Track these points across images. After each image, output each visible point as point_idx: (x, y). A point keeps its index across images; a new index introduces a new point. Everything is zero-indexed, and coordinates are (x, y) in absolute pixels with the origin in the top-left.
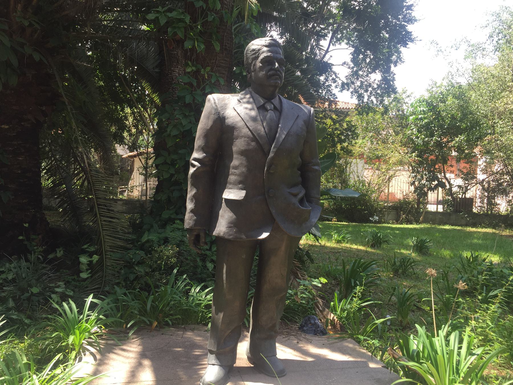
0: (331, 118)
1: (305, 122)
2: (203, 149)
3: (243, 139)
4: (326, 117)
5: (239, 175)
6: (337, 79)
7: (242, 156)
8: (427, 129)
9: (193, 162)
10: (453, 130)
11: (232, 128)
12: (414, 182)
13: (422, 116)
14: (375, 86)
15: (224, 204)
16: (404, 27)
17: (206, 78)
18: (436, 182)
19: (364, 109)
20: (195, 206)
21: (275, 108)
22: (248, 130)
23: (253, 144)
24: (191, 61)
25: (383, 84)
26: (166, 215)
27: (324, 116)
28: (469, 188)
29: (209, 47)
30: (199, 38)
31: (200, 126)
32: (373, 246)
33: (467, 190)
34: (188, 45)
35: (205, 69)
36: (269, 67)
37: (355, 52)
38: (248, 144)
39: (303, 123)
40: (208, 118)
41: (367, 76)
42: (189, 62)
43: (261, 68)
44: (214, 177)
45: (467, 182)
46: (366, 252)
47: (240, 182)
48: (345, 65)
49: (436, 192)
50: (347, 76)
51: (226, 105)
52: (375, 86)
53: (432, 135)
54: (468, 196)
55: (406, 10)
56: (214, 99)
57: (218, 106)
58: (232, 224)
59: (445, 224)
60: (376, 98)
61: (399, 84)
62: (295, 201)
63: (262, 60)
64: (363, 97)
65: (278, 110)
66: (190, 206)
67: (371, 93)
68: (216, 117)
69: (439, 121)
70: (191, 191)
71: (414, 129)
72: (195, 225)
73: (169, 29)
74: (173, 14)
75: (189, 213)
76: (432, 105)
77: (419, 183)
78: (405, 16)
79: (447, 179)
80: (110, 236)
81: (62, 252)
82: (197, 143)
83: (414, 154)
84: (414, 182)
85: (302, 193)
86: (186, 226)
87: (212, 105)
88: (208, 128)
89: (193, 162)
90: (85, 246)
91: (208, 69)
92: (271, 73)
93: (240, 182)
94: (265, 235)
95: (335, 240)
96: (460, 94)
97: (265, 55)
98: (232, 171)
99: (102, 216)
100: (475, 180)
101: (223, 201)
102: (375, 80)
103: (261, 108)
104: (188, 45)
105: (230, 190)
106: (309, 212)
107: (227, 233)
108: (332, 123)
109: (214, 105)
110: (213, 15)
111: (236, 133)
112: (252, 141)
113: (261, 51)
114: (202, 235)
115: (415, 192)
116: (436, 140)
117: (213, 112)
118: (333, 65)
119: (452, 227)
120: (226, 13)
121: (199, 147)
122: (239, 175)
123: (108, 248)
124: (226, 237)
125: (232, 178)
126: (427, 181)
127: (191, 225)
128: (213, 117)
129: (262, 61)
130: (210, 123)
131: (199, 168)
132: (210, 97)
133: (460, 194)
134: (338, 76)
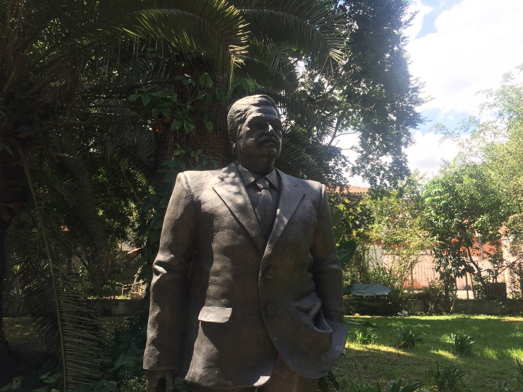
0: (344, 203)
1: (314, 202)
2: (170, 248)
3: (226, 231)
4: (338, 202)
5: (221, 285)
6: (347, 163)
7: (225, 255)
8: (446, 210)
9: (157, 267)
10: (474, 211)
12: (439, 268)
13: (439, 197)
14: (387, 169)
15: (200, 330)
16: (411, 109)
17: (198, 161)
18: (463, 267)
19: (377, 193)
20: (157, 335)
21: (270, 184)
22: (233, 218)
23: (241, 237)
24: (180, 144)
25: (395, 166)
27: (336, 201)
28: (499, 271)
29: (200, 127)
30: (189, 118)
31: (167, 215)
32: (404, 347)
33: (497, 274)
34: (176, 126)
35: (196, 152)
36: (260, 132)
37: (363, 135)
38: (234, 238)
39: (311, 204)
40: (177, 204)
41: (378, 159)
42: (178, 145)
43: (248, 134)
44: (185, 289)
45: (496, 265)
46: (399, 355)
47: (223, 296)
48: (354, 149)
49: (464, 277)
50: (356, 161)
51: (202, 184)
52: (387, 169)
53: (452, 217)
54: (500, 280)
55: (412, 92)
56: (186, 179)
57: (192, 187)
58: (212, 363)
59: (478, 314)
60: (389, 180)
61: (411, 166)
62: (308, 320)
63: (249, 122)
64: (376, 181)
65: (276, 189)
66: (151, 334)
67: (383, 176)
68: (188, 201)
69: (457, 202)
70: (153, 310)
71: (433, 211)
72: (158, 364)
73: (153, 110)
74: (158, 94)
75: (150, 345)
76: (448, 185)
77: (445, 269)
78: (411, 98)
79: (474, 263)
80: (74, 362)
81: (19, 383)
82: (162, 240)
83: (435, 238)
84: (439, 268)
85: (317, 306)
86: (145, 367)
87: (182, 185)
88: (178, 217)
89: (157, 267)
90: (44, 376)
91: (200, 151)
92: (263, 138)
93: (223, 296)
94: (263, 380)
95: (361, 340)
96: (476, 174)
97: (255, 115)
98: (212, 278)
99: (66, 335)
101: (200, 325)
102: (386, 163)
103: (251, 188)
104: (176, 126)
105: (209, 308)
106: (330, 336)
107: (205, 376)
108: (345, 208)
109: (185, 186)
110: (204, 93)
111: (216, 224)
112: (239, 234)
113: (248, 112)
114: (169, 380)
115: (441, 278)
116: (457, 221)
117: (184, 195)
118: (341, 149)
119: (489, 317)
120: (219, 91)
121: (165, 245)
122: (221, 285)
123: (70, 379)
124: (204, 384)
125: (212, 289)
126: (453, 266)
127: (151, 365)
129: (250, 124)
130: (180, 210)
131: (164, 275)
132: (181, 175)
133: (490, 279)
134: (348, 159)
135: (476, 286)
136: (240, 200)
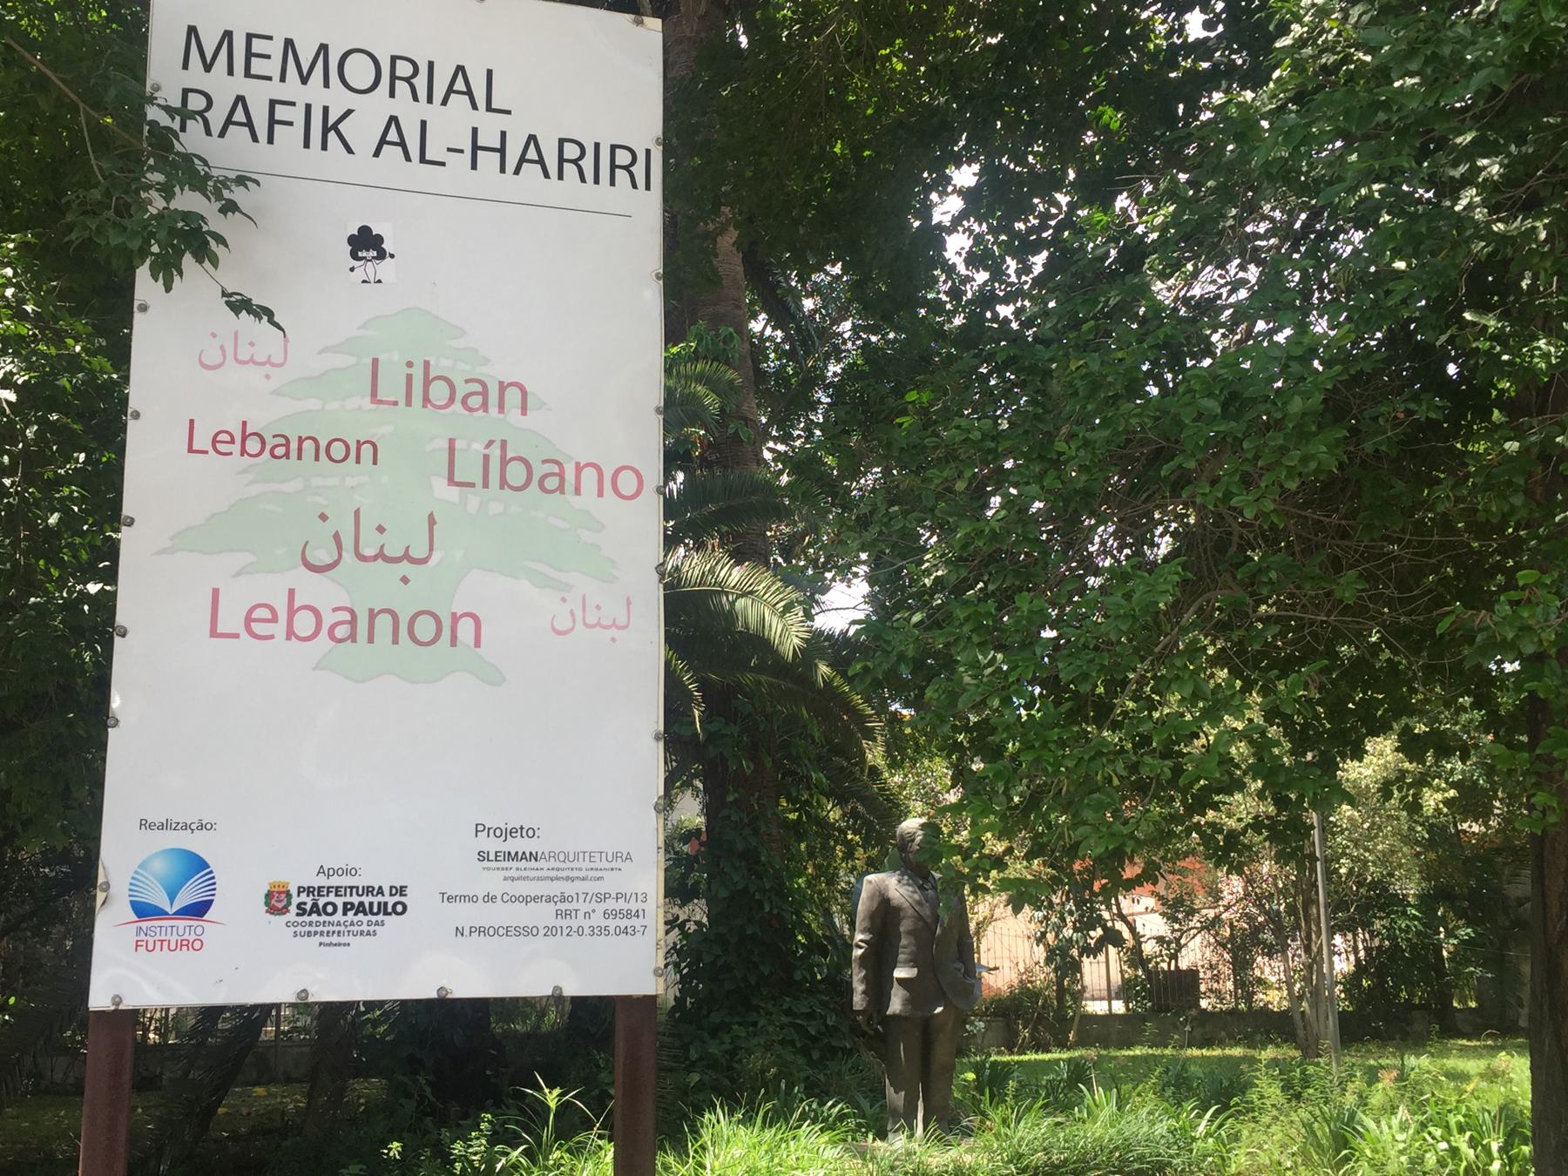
11: (898, 909)
12: (1044, 934)
18: (1099, 931)
26: (716, 1018)
28: (1183, 941)
33: (1180, 947)
45: (1177, 926)
49: (1101, 957)
54: (1184, 964)
58: (906, 1002)
59: (1129, 1046)
77: (1057, 936)
79: (1123, 918)
84: (1044, 934)
94: (939, 1010)
100: (1196, 918)
103: (921, 888)
115: (1048, 961)
125: (901, 957)
126: (1075, 930)
128: (871, 898)
135: (1129, 980)
136: (916, 897)
